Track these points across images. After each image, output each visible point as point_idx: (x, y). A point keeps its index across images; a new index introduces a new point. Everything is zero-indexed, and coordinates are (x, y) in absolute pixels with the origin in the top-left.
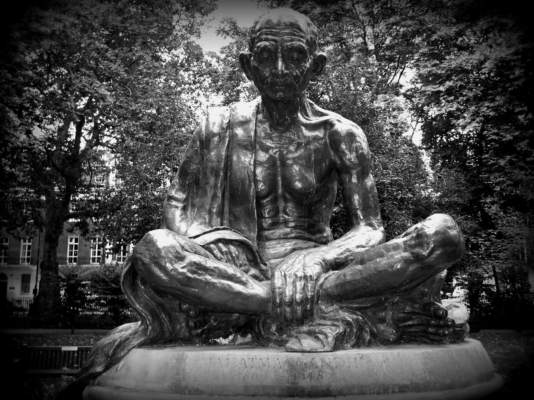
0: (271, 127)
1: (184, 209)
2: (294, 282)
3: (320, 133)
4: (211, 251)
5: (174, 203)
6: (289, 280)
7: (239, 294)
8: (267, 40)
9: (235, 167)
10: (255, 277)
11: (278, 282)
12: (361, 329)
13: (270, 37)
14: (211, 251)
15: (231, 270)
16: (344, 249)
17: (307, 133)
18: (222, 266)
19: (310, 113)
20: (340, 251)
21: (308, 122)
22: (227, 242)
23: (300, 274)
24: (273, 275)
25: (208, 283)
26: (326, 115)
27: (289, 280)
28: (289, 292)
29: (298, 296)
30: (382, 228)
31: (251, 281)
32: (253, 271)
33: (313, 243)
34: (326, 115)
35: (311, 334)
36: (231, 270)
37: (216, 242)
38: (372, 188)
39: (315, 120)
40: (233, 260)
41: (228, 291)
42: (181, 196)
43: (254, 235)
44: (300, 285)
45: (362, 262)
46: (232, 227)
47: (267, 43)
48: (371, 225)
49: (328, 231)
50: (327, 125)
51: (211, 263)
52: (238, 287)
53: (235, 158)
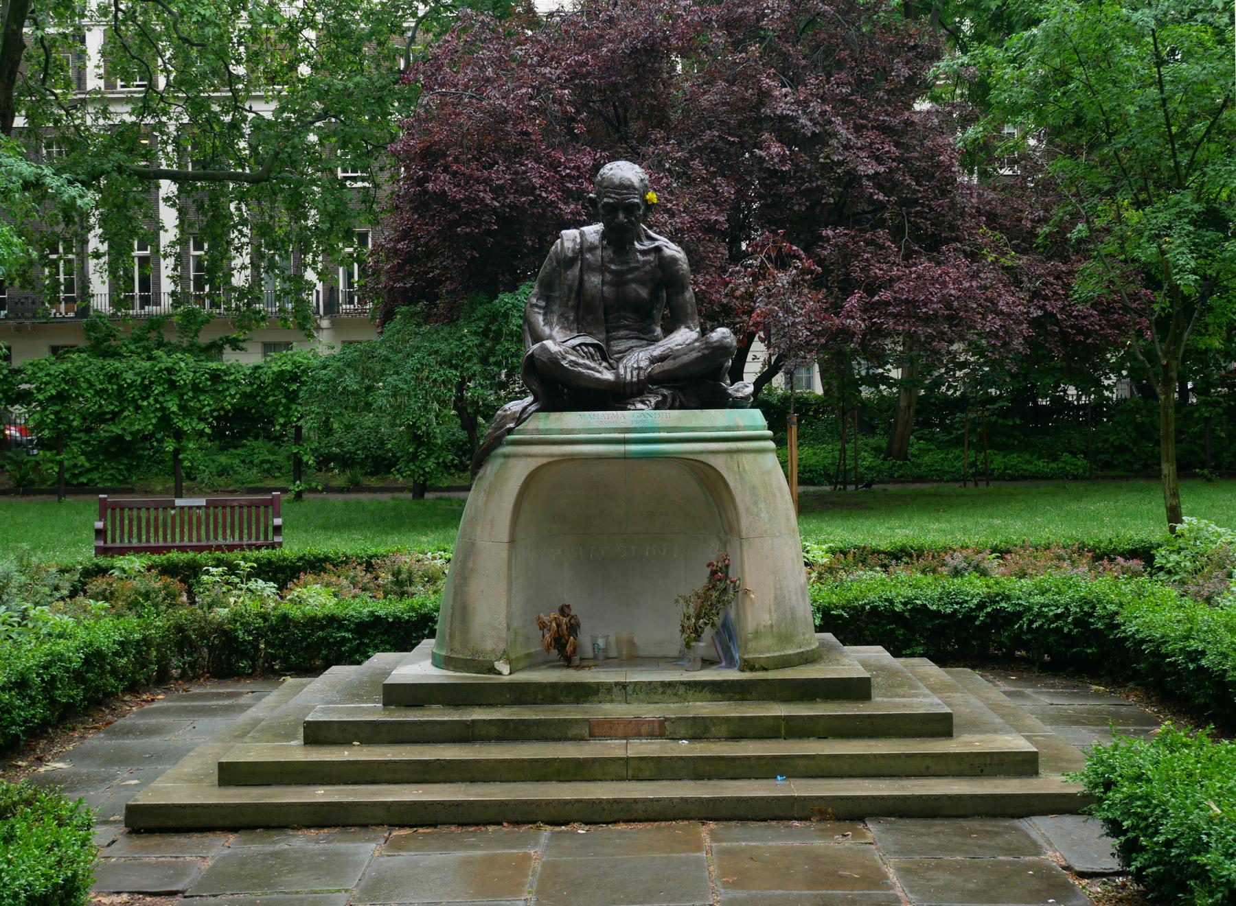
0: (614, 252)
1: (545, 314)
2: (632, 372)
3: (651, 258)
4: (577, 351)
5: (537, 310)
6: (628, 370)
7: (598, 379)
8: (609, 197)
9: (587, 285)
10: (605, 367)
11: (622, 371)
12: (674, 400)
13: (613, 195)
14: (577, 351)
15: (592, 365)
16: (666, 347)
17: (640, 257)
18: (587, 362)
19: (644, 238)
20: (662, 349)
21: (642, 247)
22: (586, 345)
23: (635, 366)
24: (618, 367)
25: (580, 373)
26: (657, 240)
27: (628, 370)
28: (629, 377)
29: (635, 379)
30: (698, 329)
31: (605, 371)
32: (604, 364)
33: (645, 342)
34: (657, 240)
35: (643, 402)
36: (592, 365)
37: (580, 345)
38: (691, 298)
39: (648, 245)
40: (592, 357)
41: (590, 378)
42: (543, 304)
43: (602, 336)
44: (635, 373)
45: (674, 359)
46: (590, 334)
47: (611, 201)
48: (688, 327)
49: (658, 330)
50: (658, 250)
51: (581, 361)
52: (597, 375)
53: (586, 278)
